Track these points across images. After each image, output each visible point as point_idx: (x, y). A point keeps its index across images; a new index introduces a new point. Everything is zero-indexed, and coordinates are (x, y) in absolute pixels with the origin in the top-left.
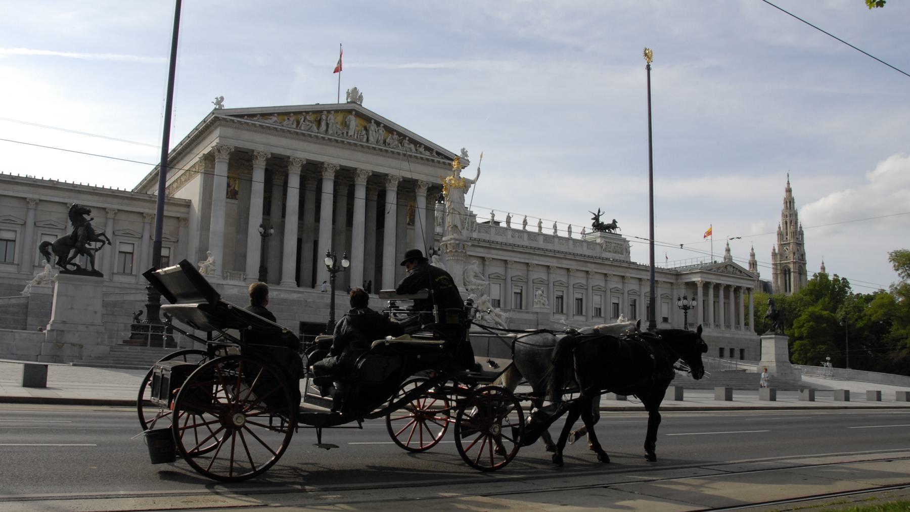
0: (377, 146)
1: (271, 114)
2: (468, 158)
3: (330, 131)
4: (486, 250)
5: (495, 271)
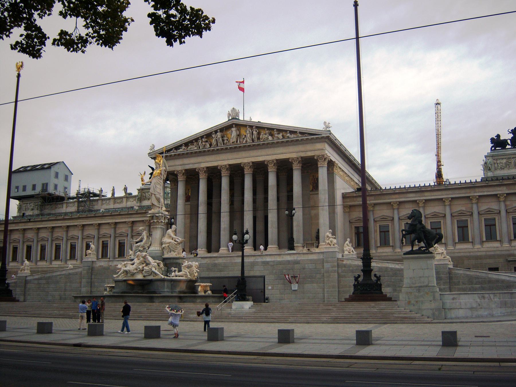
0: (251, 144)
1: (181, 146)
2: (330, 129)
3: (219, 144)
4: (418, 194)
5: (433, 211)
